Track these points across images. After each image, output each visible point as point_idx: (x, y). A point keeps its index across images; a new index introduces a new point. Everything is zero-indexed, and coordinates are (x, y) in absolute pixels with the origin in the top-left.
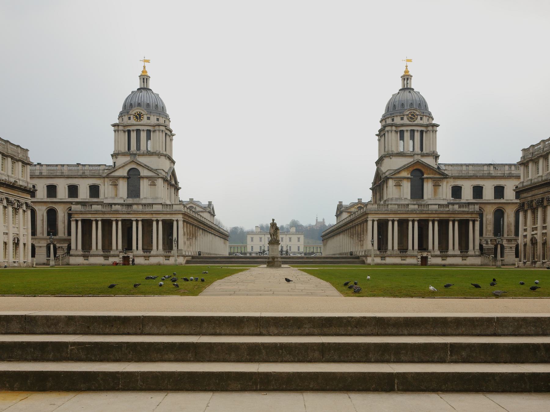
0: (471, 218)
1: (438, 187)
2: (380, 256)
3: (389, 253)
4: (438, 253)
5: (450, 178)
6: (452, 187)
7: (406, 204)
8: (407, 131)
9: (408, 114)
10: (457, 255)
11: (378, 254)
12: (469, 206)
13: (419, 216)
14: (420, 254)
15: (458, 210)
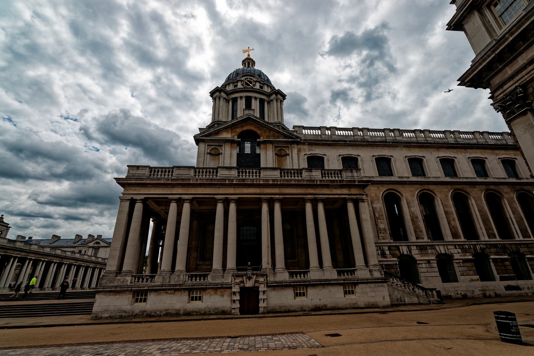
0: (349, 195)
1: (284, 158)
2: (131, 291)
3: (158, 280)
4: (284, 276)
5: (303, 144)
6: (307, 157)
7: (213, 168)
8: (241, 97)
9: (243, 80)
10: (331, 280)
11: (129, 283)
12: (341, 174)
13: (238, 191)
14: (238, 280)
15: (321, 179)
